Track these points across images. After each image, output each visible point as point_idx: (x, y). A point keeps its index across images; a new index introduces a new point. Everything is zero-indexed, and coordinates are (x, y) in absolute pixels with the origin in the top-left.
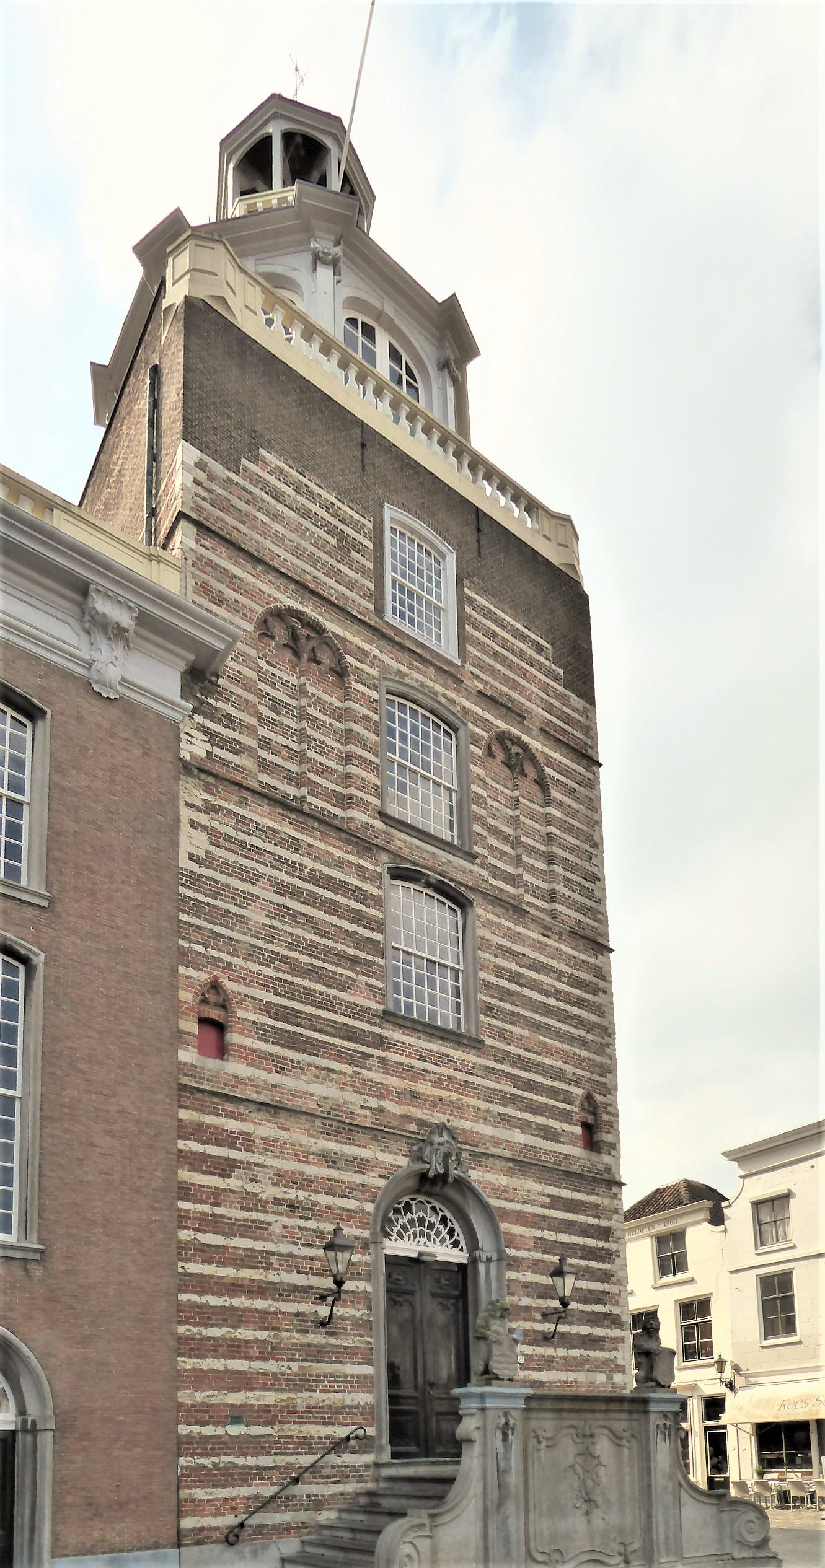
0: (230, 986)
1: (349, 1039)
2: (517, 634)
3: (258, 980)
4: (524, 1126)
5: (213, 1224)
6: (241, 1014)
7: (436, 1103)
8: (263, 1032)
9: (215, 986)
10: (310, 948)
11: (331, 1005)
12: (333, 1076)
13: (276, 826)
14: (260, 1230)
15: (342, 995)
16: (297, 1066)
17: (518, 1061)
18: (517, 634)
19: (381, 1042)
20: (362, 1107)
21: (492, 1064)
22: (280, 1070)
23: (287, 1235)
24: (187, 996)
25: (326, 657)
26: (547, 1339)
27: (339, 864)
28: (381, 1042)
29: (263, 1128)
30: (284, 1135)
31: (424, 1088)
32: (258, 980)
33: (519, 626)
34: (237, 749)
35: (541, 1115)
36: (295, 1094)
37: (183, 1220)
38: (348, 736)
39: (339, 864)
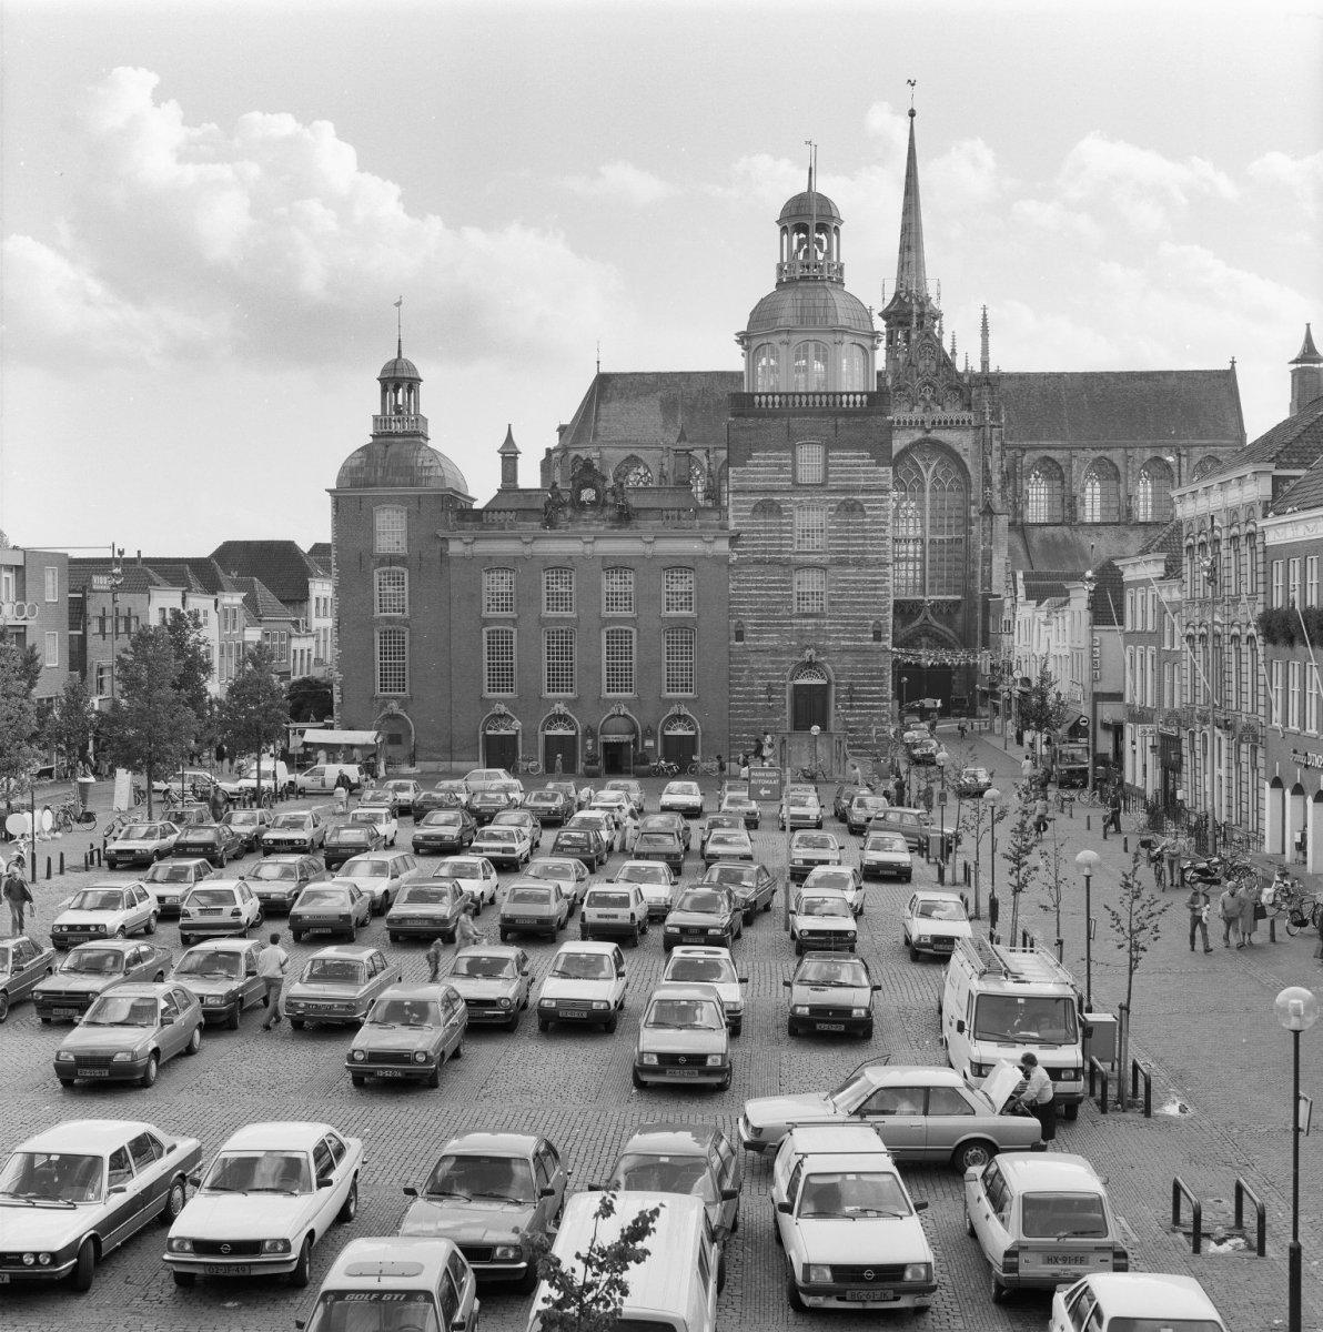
2: (855, 457)
4: (844, 639)
5: (740, 685)
8: (753, 632)
10: (768, 603)
14: (752, 685)
17: (847, 618)
18: (855, 457)
19: (791, 624)
23: (760, 685)
24: (732, 628)
25: (775, 508)
26: (851, 707)
29: (753, 657)
34: (745, 553)
38: (782, 531)
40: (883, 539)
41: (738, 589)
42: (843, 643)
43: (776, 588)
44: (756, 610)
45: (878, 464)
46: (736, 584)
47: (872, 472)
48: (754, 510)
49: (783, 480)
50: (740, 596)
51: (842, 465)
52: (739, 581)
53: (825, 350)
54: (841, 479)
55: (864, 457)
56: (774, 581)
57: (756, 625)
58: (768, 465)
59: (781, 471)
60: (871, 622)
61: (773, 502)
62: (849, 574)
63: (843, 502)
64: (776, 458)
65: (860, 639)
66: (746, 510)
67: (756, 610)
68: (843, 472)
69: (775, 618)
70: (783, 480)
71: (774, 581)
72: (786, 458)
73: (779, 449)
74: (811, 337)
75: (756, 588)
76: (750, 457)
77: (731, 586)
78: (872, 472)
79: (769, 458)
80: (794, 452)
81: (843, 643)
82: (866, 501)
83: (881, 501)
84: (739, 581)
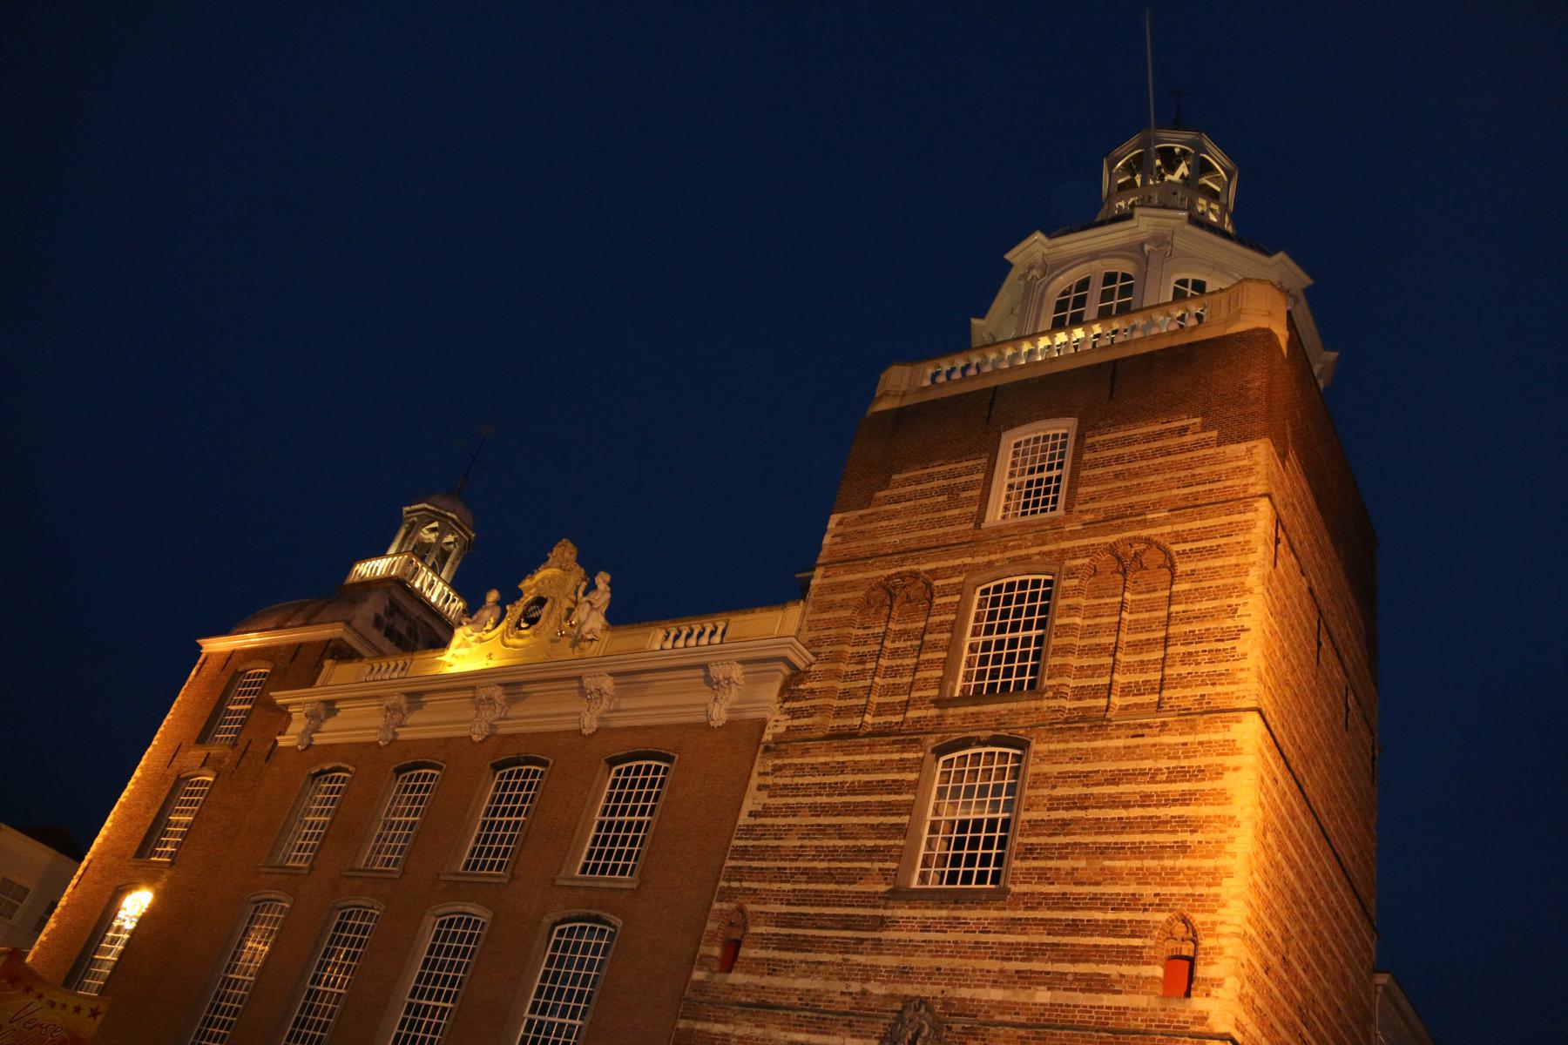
0: (751, 907)
1: (847, 928)
3: (779, 897)
6: (752, 930)
7: (933, 974)
8: (764, 941)
9: (741, 910)
11: (839, 899)
12: (821, 968)
13: (828, 759)
15: (853, 888)
16: (789, 966)
20: (843, 993)
21: (1020, 914)
22: (773, 973)
27: (881, 767)
28: (882, 923)
30: (759, 1031)
31: (921, 961)
32: (779, 897)
35: (1087, 961)
36: (780, 991)
39: (881, 767)
41: (766, 811)
42: (1043, 996)
50: (765, 831)
52: (773, 790)
57: (780, 920)
59: (954, 502)
60: (1162, 917)
62: (1098, 754)
69: (839, 899)
70: (951, 522)
75: (816, 810)
76: (885, 484)
77: (748, 805)
79: (931, 477)
81: (1043, 996)
82: (1179, 537)
84: (773, 790)
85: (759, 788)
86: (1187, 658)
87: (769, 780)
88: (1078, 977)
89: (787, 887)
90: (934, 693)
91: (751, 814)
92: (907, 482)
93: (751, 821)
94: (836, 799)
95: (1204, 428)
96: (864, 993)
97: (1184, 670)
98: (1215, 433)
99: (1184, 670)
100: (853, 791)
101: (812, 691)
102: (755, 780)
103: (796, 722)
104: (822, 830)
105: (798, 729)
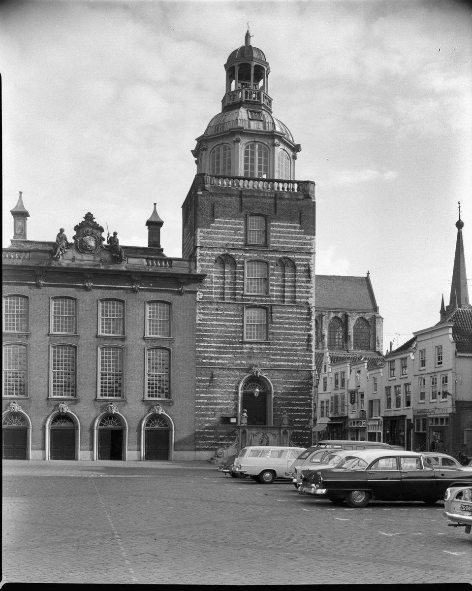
2: (288, 227)
10: (225, 332)
18: (288, 227)
22: (218, 360)
33: (289, 224)
37: (197, 392)
40: (308, 287)
41: (203, 320)
43: (231, 321)
44: (217, 337)
45: (305, 234)
46: (201, 316)
47: (301, 239)
48: (216, 262)
49: (237, 240)
50: (205, 325)
51: (280, 232)
52: (204, 314)
53: (265, 149)
54: (279, 242)
55: (295, 228)
56: (230, 315)
58: (227, 228)
59: (236, 234)
61: (231, 257)
63: (280, 260)
64: (232, 223)
65: (292, 361)
66: (209, 261)
67: (217, 337)
68: (280, 237)
70: (237, 240)
71: (230, 315)
72: (239, 224)
73: (235, 218)
74: (257, 139)
75: (217, 320)
76: (213, 222)
77: (197, 318)
78: (301, 239)
79: (227, 223)
80: (246, 221)
82: (296, 259)
83: (308, 260)
84: (204, 314)
85: (200, 313)
86: (300, 292)
87: (202, 311)
88: (286, 360)
89: (216, 339)
90: (242, 292)
91: (199, 320)
92: (220, 222)
93: (200, 322)
94: (223, 318)
95: (301, 228)
96: (241, 363)
97: (300, 295)
98: (303, 231)
99: (300, 295)
100: (226, 316)
101: (207, 287)
102: (198, 311)
103: (205, 295)
104: (221, 325)
105: (206, 297)
